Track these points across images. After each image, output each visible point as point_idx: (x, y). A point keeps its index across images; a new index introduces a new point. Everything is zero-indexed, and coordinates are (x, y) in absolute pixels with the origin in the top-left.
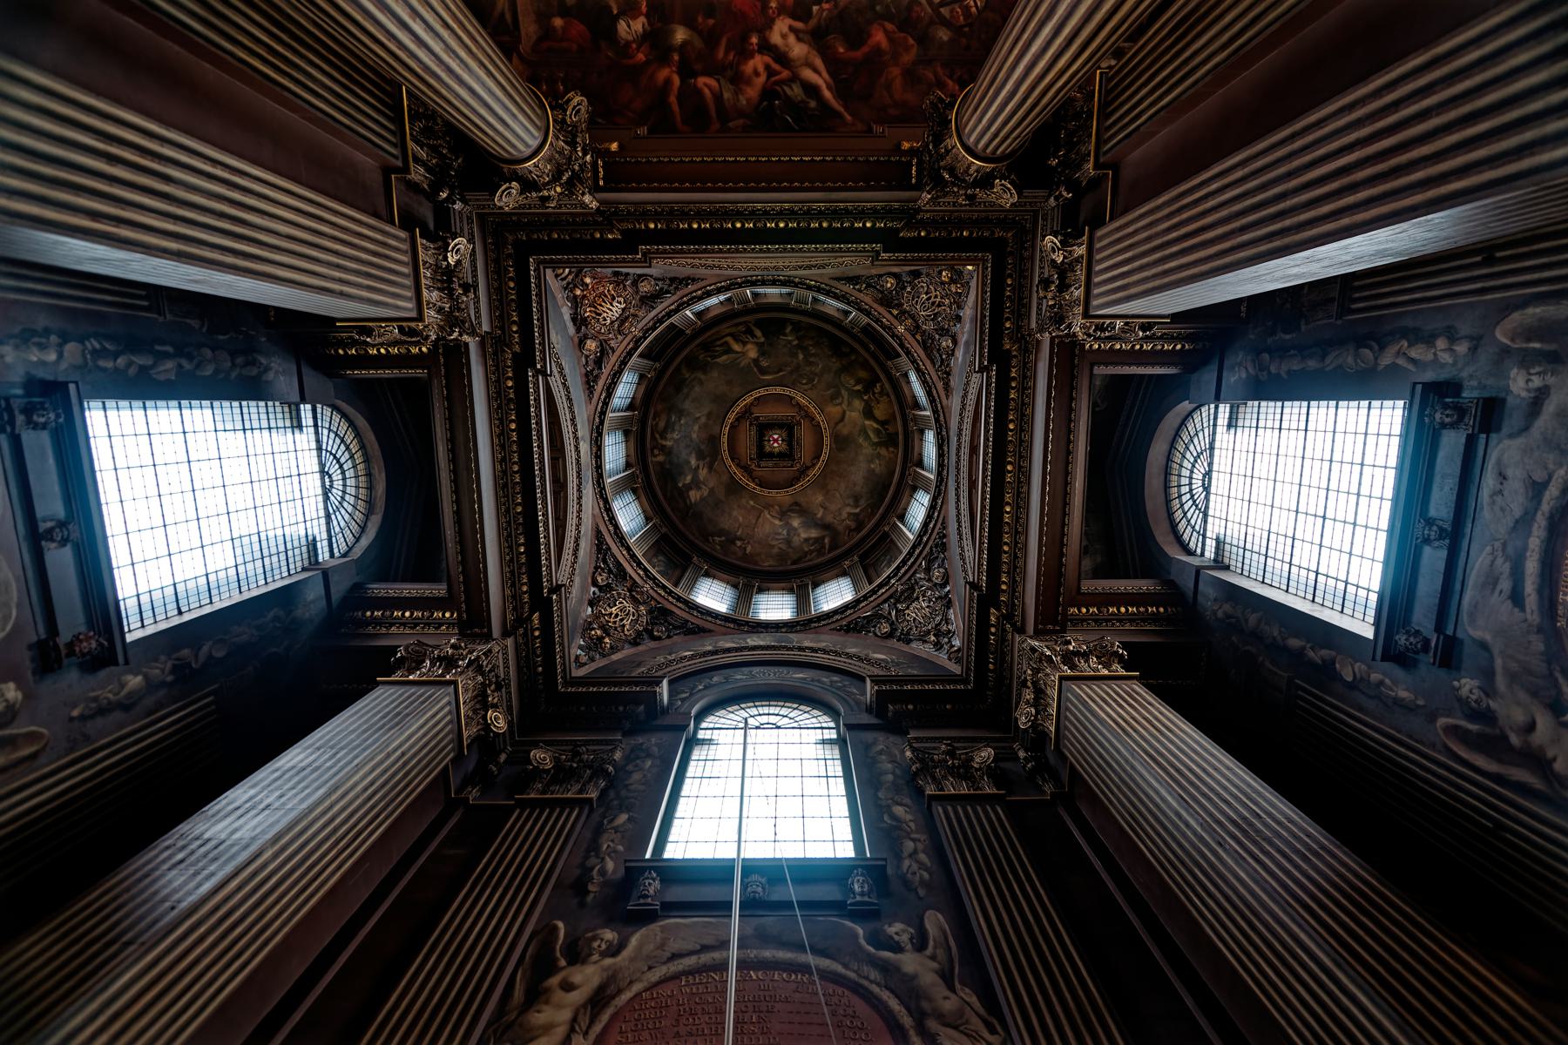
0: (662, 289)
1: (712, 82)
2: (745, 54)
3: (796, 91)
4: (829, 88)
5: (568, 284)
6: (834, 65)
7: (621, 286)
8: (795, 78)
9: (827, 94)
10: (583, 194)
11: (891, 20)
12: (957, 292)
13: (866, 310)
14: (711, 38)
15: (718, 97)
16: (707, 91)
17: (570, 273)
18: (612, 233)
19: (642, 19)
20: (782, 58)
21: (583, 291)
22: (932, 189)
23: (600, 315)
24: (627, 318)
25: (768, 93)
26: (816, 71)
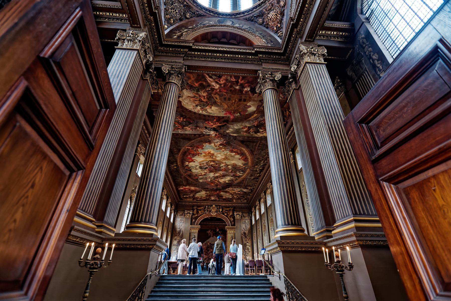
0: (256, 18)
1: (232, 80)
2: (225, 84)
3: (214, 77)
4: (207, 77)
5: (280, 29)
6: (206, 81)
7: (267, 23)
8: (214, 79)
9: (207, 76)
10: (261, 77)
11: (194, 87)
12: (168, 15)
13: (194, 3)
14: (231, 86)
15: (231, 77)
16: (233, 78)
17: (278, 33)
18: (260, 57)
19: (244, 90)
20: (217, 83)
21: (278, 25)
22: (182, 72)
23: (276, 14)
24: (269, 10)
25: (220, 77)
26: (210, 80)
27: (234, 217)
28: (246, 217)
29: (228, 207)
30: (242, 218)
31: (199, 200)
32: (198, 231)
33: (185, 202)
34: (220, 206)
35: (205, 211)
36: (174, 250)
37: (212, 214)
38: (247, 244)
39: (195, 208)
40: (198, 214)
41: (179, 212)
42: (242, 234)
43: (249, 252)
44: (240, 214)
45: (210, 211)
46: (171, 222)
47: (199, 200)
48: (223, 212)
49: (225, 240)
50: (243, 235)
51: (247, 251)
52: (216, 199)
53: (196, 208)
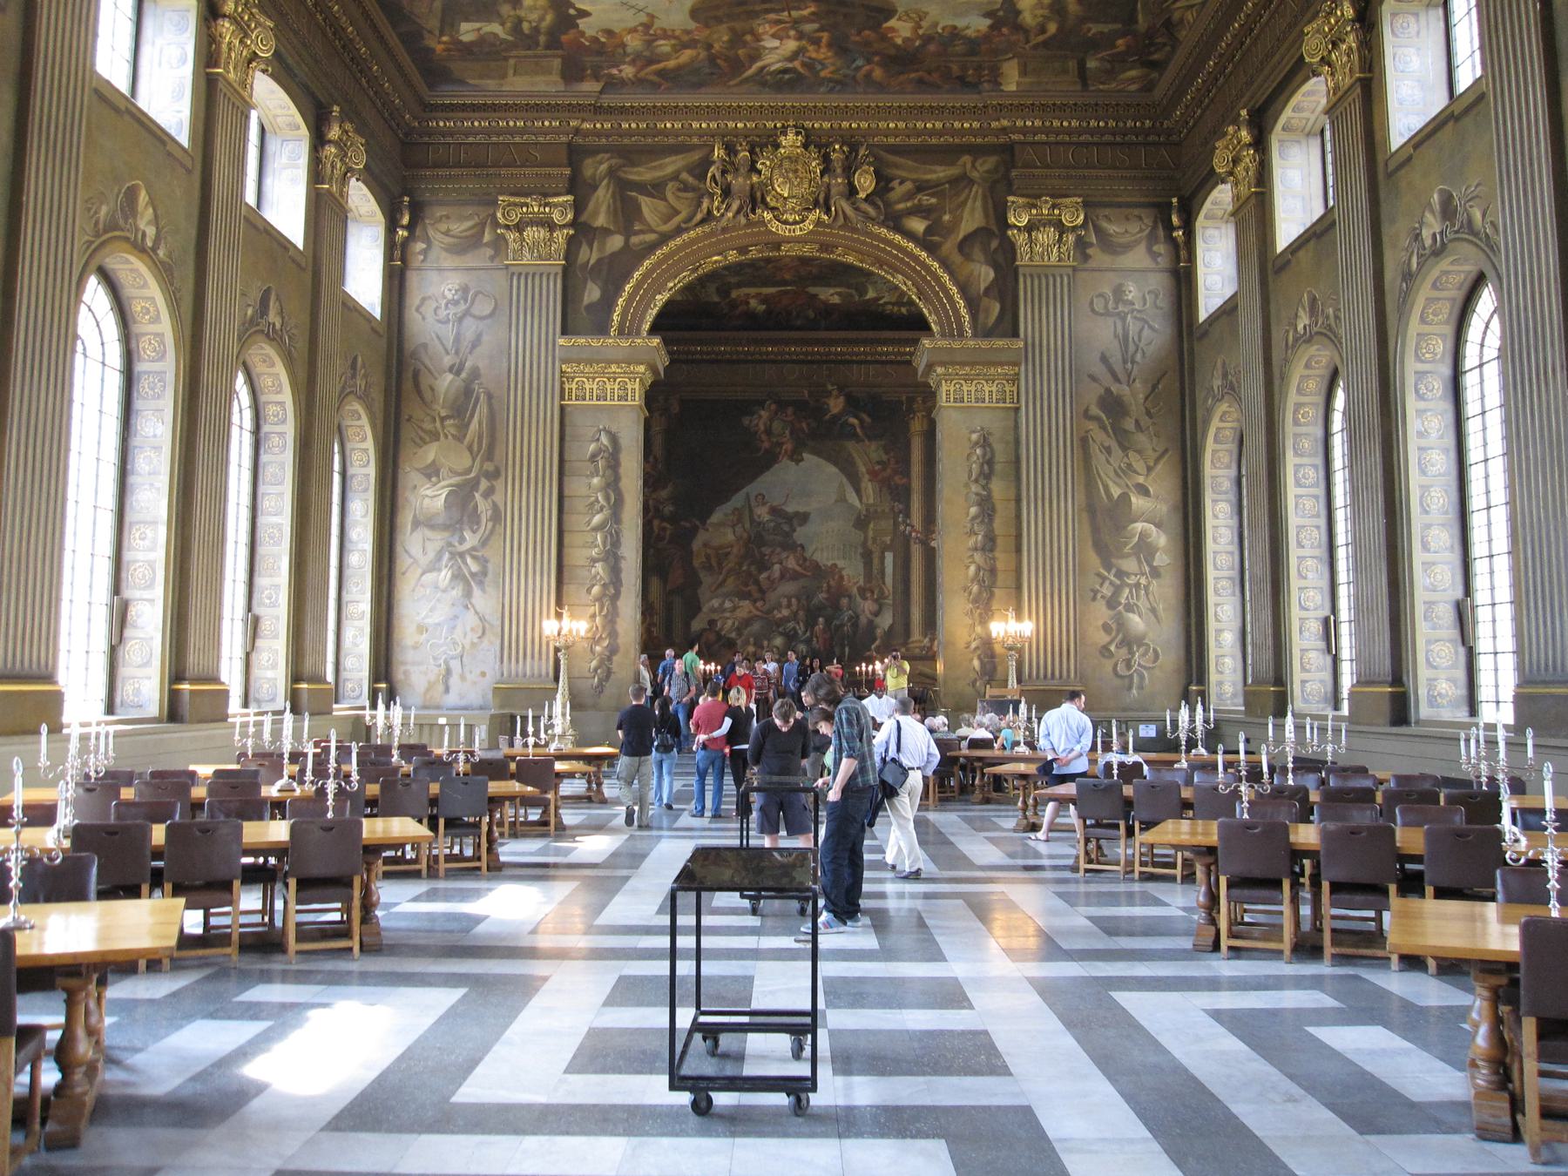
27: (1010, 249)
28: (1127, 247)
29: (947, 154)
30: (1086, 257)
31: (639, 82)
32: (653, 396)
33: (494, 108)
34: (854, 148)
35: (701, 194)
36: (424, 561)
37: (775, 226)
38: (1137, 501)
39: (596, 167)
40: (628, 232)
41: (440, 212)
42: (1087, 415)
43: (1155, 572)
44: (1066, 219)
45: (756, 199)
46: (351, 307)
47: (639, 82)
48: (887, 204)
49: (898, 480)
50: (1092, 426)
51: (1130, 565)
52: (810, 65)
53: (611, 172)
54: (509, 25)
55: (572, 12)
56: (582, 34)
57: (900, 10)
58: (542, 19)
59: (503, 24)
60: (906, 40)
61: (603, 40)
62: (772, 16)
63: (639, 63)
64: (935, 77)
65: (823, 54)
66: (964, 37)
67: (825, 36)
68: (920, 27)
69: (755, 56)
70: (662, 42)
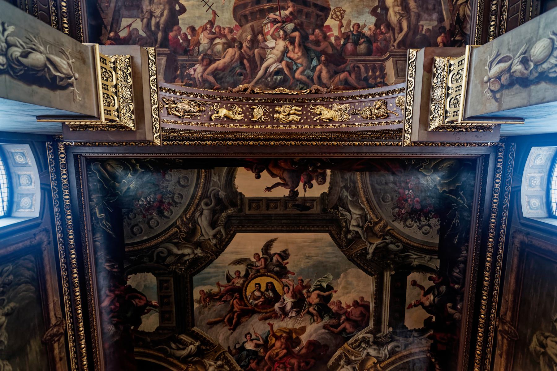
54: (145, 20)
55: (177, 8)
56: (180, 29)
57: (332, 8)
58: (162, 14)
59: (142, 21)
60: (337, 38)
61: (189, 37)
62: (271, 15)
63: (205, 63)
64: (353, 76)
65: (296, 54)
66: (364, 36)
67: (297, 34)
68: (342, 26)
69: (263, 59)
70: (218, 41)
